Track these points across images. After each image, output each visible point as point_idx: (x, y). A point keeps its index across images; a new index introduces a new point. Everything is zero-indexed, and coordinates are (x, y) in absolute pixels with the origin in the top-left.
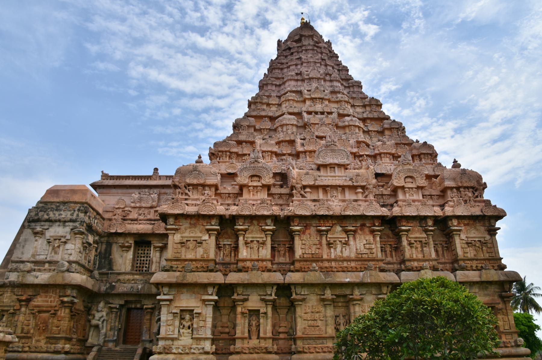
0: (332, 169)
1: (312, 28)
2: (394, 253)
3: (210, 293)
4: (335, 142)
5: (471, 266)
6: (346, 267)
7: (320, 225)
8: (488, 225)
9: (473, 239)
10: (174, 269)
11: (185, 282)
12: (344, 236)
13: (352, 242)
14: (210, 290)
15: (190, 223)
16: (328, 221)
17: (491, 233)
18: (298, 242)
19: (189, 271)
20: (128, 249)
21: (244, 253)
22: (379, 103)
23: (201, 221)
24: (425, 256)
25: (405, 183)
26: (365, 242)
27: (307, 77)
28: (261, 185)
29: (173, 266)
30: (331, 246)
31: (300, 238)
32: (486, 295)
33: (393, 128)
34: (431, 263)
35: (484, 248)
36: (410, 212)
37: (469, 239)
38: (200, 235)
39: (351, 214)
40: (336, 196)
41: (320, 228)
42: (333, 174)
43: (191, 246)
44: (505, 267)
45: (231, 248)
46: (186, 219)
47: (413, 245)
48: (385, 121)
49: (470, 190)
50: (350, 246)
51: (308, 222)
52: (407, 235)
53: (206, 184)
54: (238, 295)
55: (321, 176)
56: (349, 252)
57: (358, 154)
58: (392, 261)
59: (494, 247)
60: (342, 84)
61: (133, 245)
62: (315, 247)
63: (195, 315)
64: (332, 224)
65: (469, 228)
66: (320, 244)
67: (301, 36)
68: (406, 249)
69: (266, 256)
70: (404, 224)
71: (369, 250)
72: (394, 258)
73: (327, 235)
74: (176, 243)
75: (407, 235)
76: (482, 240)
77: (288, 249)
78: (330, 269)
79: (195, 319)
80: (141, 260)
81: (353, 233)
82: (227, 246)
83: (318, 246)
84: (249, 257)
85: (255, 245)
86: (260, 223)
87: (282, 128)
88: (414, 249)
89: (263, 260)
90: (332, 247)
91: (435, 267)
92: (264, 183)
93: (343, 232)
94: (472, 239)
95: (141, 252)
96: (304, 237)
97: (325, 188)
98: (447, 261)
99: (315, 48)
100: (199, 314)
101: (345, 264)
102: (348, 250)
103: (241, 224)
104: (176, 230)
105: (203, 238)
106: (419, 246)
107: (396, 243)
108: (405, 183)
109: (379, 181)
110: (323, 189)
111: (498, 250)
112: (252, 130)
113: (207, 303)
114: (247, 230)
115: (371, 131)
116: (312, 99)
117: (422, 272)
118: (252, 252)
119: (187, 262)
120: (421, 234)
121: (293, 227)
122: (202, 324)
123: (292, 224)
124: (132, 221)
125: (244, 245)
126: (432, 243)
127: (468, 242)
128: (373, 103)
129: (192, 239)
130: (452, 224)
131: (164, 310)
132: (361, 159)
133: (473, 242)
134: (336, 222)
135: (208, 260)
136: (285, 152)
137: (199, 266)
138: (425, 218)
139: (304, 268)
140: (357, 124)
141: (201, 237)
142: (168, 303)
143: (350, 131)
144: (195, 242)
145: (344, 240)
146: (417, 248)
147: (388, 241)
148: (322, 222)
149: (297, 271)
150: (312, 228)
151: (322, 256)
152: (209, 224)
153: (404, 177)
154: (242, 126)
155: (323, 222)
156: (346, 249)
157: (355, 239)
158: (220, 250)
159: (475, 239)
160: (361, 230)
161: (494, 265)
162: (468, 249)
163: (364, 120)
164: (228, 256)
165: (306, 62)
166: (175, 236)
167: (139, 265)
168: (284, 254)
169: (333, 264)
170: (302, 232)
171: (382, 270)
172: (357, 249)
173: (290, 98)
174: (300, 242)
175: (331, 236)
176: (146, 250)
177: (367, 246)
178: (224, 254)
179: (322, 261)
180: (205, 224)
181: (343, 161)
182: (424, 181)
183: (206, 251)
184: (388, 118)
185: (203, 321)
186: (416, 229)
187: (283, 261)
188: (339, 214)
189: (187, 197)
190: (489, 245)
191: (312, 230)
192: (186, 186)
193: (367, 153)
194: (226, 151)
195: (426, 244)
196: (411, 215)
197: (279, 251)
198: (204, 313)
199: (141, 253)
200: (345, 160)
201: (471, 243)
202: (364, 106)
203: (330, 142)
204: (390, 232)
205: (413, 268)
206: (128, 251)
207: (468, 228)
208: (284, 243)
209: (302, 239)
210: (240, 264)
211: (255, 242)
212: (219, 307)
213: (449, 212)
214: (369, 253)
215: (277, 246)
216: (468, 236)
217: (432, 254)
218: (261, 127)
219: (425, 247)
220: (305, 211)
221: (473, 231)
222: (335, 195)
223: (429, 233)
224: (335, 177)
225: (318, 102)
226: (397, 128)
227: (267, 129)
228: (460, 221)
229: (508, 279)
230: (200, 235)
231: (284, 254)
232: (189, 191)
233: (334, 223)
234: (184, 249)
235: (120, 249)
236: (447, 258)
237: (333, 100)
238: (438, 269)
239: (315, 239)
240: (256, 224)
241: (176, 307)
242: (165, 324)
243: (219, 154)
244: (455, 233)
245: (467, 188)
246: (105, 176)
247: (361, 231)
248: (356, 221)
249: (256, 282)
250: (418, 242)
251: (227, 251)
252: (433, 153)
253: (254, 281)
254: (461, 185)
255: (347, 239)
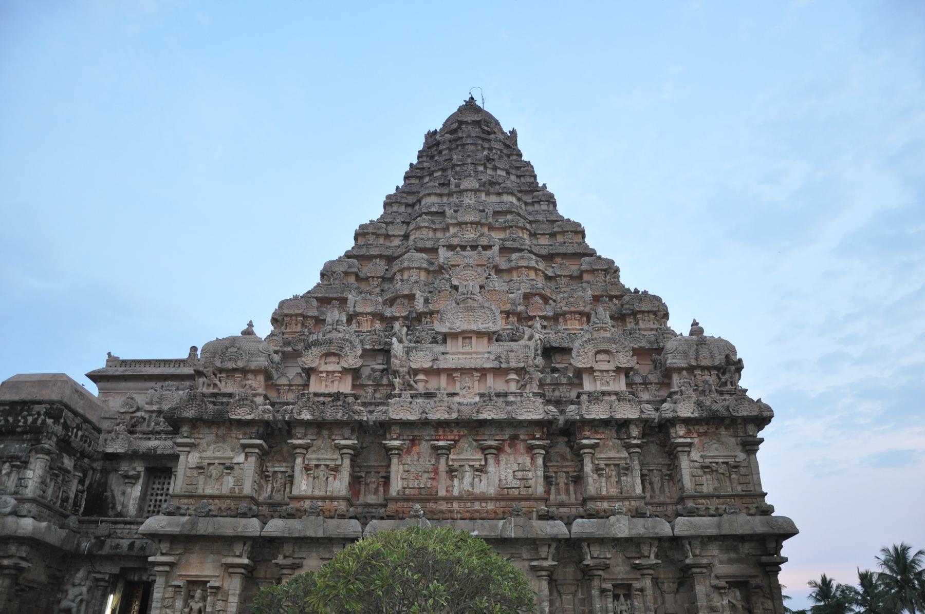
0: (467, 340)
1: (479, 110)
2: (572, 488)
3: (237, 553)
4: (474, 294)
5: (707, 509)
6: (478, 511)
7: (438, 437)
8: (742, 435)
9: (714, 460)
10: (182, 511)
11: (194, 532)
12: (478, 457)
13: (491, 468)
14: (238, 548)
15: (217, 435)
16: (452, 431)
17: (748, 448)
18: (396, 469)
19: (204, 514)
20: (134, 482)
21: (303, 486)
22: (579, 229)
23: (235, 432)
24: (624, 492)
25: (596, 362)
26: (516, 467)
27: (457, 189)
28: (340, 369)
29: (181, 506)
30: (453, 474)
31: (401, 461)
32: (731, 561)
33: (598, 270)
34: (633, 503)
35: (733, 476)
36: (597, 412)
37: (705, 461)
38: (231, 454)
39: (490, 418)
40: (469, 388)
41: (436, 442)
42: (467, 349)
43: (214, 472)
44: (771, 509)
45: (285, 477)
46: (209, 427)
47: (601, 472)
48: (587, 259)
49: (712, 373)
50: (489, 474)
51: (416, 433)
52: (593, 454)
53: (248, 368)
54: (285, 557)
55: (447, 353)
56: (486, 486)
57: (525, 315)
58: (567, 502)
59: (752, 474)
60: (519, 199)
61: (142, 474)
62: (426, 475)
63: (209, 591)
64: (459, 435)
65: (708, 440)
66: (436, 471)
67: (461, 123)
68: (590, 480)
69: (339, 491)
70: (588, 434)
71: (523, 481)
72: (573, 496)
73: (448, 455)
74: (190, 468)
75: (593, 454)
76: (731, 461)
77: (383, 480)
78: (449, 515)
79: (209, 598)
80: (156, 500)
81: (495, 451)
82: (280, 476)
83: (432, 475)
84: (309, 493)
85: (322, 472)
86: (332, 435)
87: (402, 275)
88: (604, 480)
89: (332, 499)
90: (456, 476)
91: (639, 511)
92: (346, 366)
93: (477, 450)
94: (711, 460)
95: (158, 486)
96: (408, 459)
97: (450, 373)
98: (668, 500)
99: (480, 142)
100: (218, 588)
101: (477, 506)
102: (484, 481)
103: (299, 436)
104: (192, 446)
105: (235, 461)
106: (614, 473)
107: (577, 470)
108: (596, 362)
109: (559, 361)
110: (448, 375)
111: (759, 478)
112: (352, 279)
113: (231, 570)
114: (310, 447)
115: (560, 276)
116: (460, 224)
117: (612, 519)
118: (317, 484)
119: (205, 501)
120: (618, 452)
121: (387, 442)
122: (220, 605)
123: (388, 437)
124: (144, 434)
125: (304, 472)
126: (638, 467)
127: (704, 465)
128: (568, 229)
129: (217, 461)
130: (676, 433)
131: (160, 581)
132: (530, 323)
133: (714, 464)
134: (466, 432)
135: (240, 497)
136: (398, 315)
137: (223, 506)
138: (625, 424)
139: (403, 512)
140: (533, 264)
141: (232, 458)
142: (167, 568)
143: (519, 277)
144: (222, 467)
145: (478, 463)
146: (608, 477)
147: (562, 466)
148: (441, 433)
149: (390, 517)
150: (424, 443)
151: (437, 491)
152: (247, 436)
153: (593, 351)
154: (335, 272)
155: (443, 432)
156: (481, 480)
157: (498, 461)
158: (267, 481)
159: (717, 460)
160: (510, 446)
161: (750, 506)
162: (704, 478)
163: (549, 258)
164: (279, 491)
165: (460, 165)
166: (190, 456)
167: (152, 507)
168: (377, 490)
169: (456, 506)
170: (405, 450)
171: (541, 517)
172: (500, 480)
173: (422, 224)
174: (401, 467)
175: (455, 457)
176: (166, 483)
177: (520, 474)
178: (273, 488)
179: (437, 499)
180: (241, 437)
181: (487, 326)
182: (629, 358)
183: (239, 482)
184: (592, 253)
185: (223, 600)
186: (611, 443)
187: (373, 502)
188: (468, 417)
189: (215, 391)
190: (743, 470)
191: (424, 447)
192: (216, 372)
193: (541, 314)
194: (297, 315)
195: (627, 469)
196: (597, 417)
197: (367, 484)
198: (226, 586)
199: (158, 489)
200: (490, 324)
201: (708, 467)
202: (553, 235)
203: (464, 294)
204: (568, 450)
205: (598, 512)
206: (134, 484)
207: (705, 439)
208: (376, 470)
209: (403, 462)
210: (294, 505)
211: (322, 467)
212: (257, 578)
213: (669, 411)
214: (522, 486)
215: (363, 474)
216: (703, 454)
217: (636, 487)
218: (369, 275)
219: (626, 475)
220: (409, 413)
221: (715, 446)
222: (468, 385)
223: (632, 450)
224: (471, 353)
225: (469, 229)
226: (605, 270)
227: (378, 277)
228: (691, 428)
229: (771, 531)
230: (231, 454)
231: (377, 490)
232: (220, 381)
233: (462, 433)
234: (202, 478)
235: (121, 481)
236: (669, 495)
237: (497, 225)
238: (646, 513)
239: (427, 463)
240: (326, 437)
241: (181, 576)
242: (159, 605)
243: (285, 319)
244: (679, 449)
245: (708, 368)
246: (112, 360)
247: (511, 448)
248: (502, 431)
249: (313, 535)
250: (612, 466)
251: (278, 483)
252: (659, 311)
253: (310, 533)
254: (695, 364)
255: (483, 463)
